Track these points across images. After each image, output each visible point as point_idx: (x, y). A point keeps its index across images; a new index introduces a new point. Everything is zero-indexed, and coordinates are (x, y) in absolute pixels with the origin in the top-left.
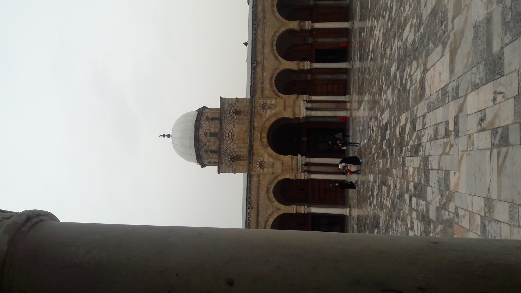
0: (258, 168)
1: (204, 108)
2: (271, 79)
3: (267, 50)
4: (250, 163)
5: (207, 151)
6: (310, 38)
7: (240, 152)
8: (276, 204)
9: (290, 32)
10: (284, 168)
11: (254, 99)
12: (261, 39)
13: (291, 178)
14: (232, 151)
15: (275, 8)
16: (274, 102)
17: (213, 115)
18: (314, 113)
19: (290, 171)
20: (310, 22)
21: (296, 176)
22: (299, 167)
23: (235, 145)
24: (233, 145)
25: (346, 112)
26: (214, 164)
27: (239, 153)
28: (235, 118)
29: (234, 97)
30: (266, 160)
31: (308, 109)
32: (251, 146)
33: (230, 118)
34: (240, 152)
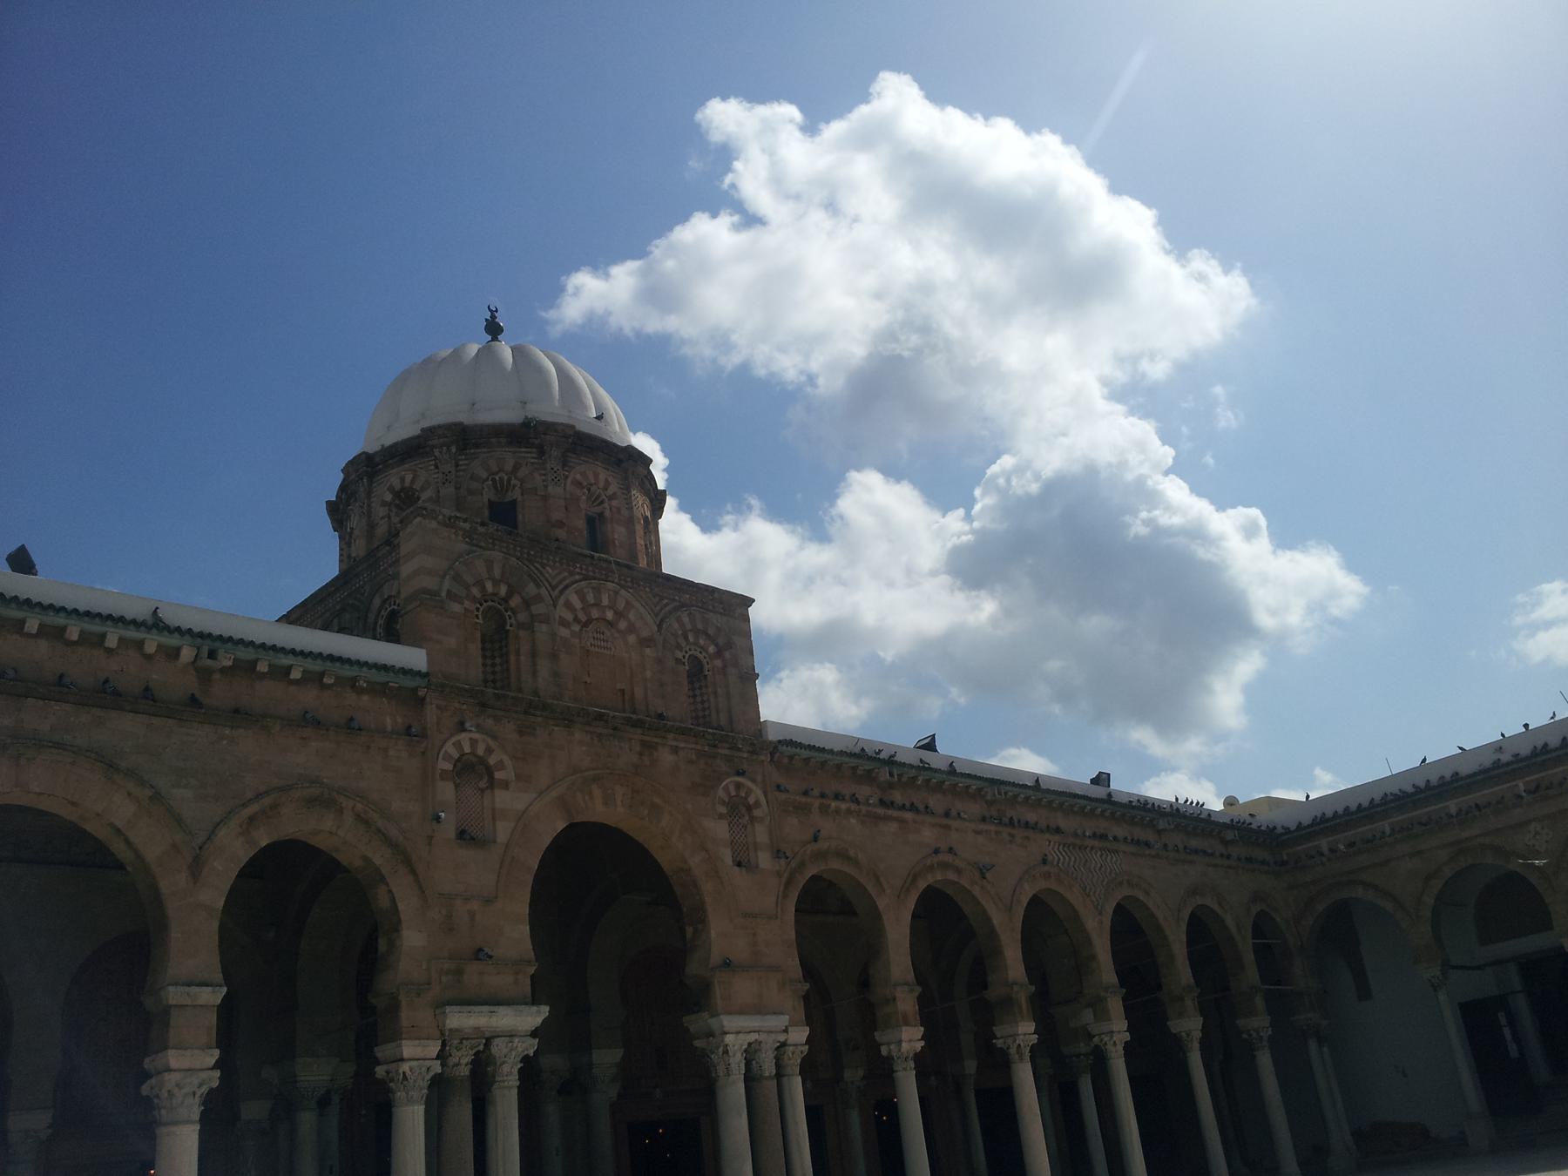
0: (458, 745)
2: (842, 854)
6: (861, 1073)
7: (534, 654)
8: (233, 852)
11: (765, 757)
16: (764, 860)
23: (564, 632)
24: (564, 623)
30: (502, 798)
31: (750, 1053)
33: (676, 626)
34: (534, 654)
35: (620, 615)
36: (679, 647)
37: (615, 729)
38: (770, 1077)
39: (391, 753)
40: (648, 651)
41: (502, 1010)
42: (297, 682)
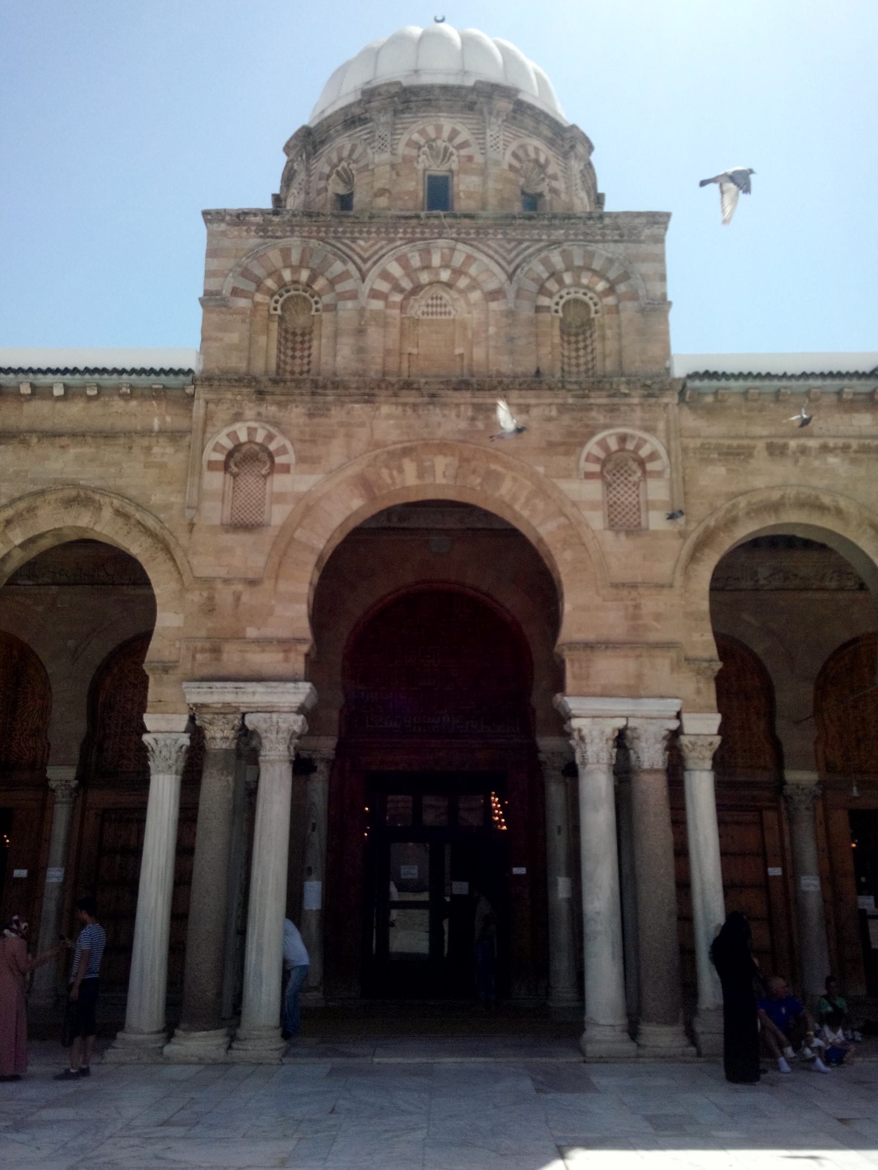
7: (336, 335)
10: (224, 595)
11: (671, 399)
13: (155, 644)
14: (339, 288)
16: (656, 521)
23: (377, 305)
24: (375, 294)
25: (621, 1021)
27: (327, 330)
28: (545, 301)
29: (675, 289)
30: (279, 482)
31: (622, 741)
33: (540, 270)
34: (336, 335)
35: (458, 272)
36: (543, 290)
37: (433, 396)
38: (652, 771)
39: (156, 450)
40: (493, 305)
42: (59, 399)
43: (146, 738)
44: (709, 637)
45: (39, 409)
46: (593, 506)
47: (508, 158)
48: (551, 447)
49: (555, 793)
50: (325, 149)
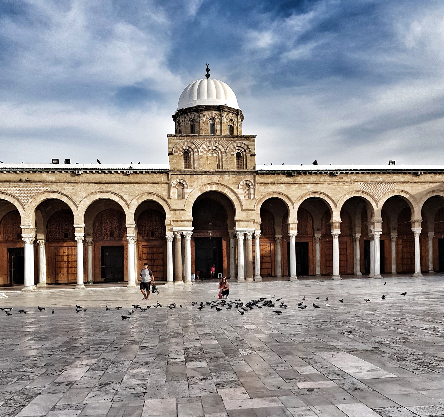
1: (242, 118)
3: (310, 188)
4: (181, 173)
5: (193, 121)
6: (320, 235)
8: (135, 204)
9: (328, 213)
12: (321, 180)
15: (354, 195)
17: (235, 127)
18: (241, 242)
19: (174, 219)
20: (340, 233)
21: (169, 225)
22: (179, 229)
24: (201, 152)
26: (178, 130)
28: (232, 153)
31: (245, 235)
32: (202, 173)
33: (232, 147)
41: (184, 228)
43: (166, 236)
44: (260, 217)
45: (140, 176)
46: (241, 194)
47: (226, 120)
48: (234, 183)
49: (232, 241)
50: (188, 114)
